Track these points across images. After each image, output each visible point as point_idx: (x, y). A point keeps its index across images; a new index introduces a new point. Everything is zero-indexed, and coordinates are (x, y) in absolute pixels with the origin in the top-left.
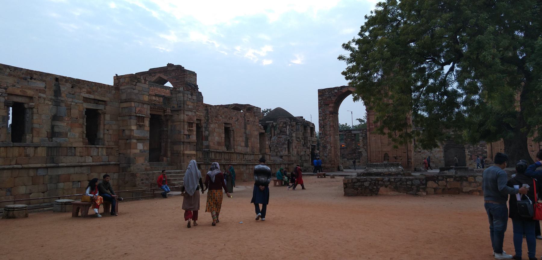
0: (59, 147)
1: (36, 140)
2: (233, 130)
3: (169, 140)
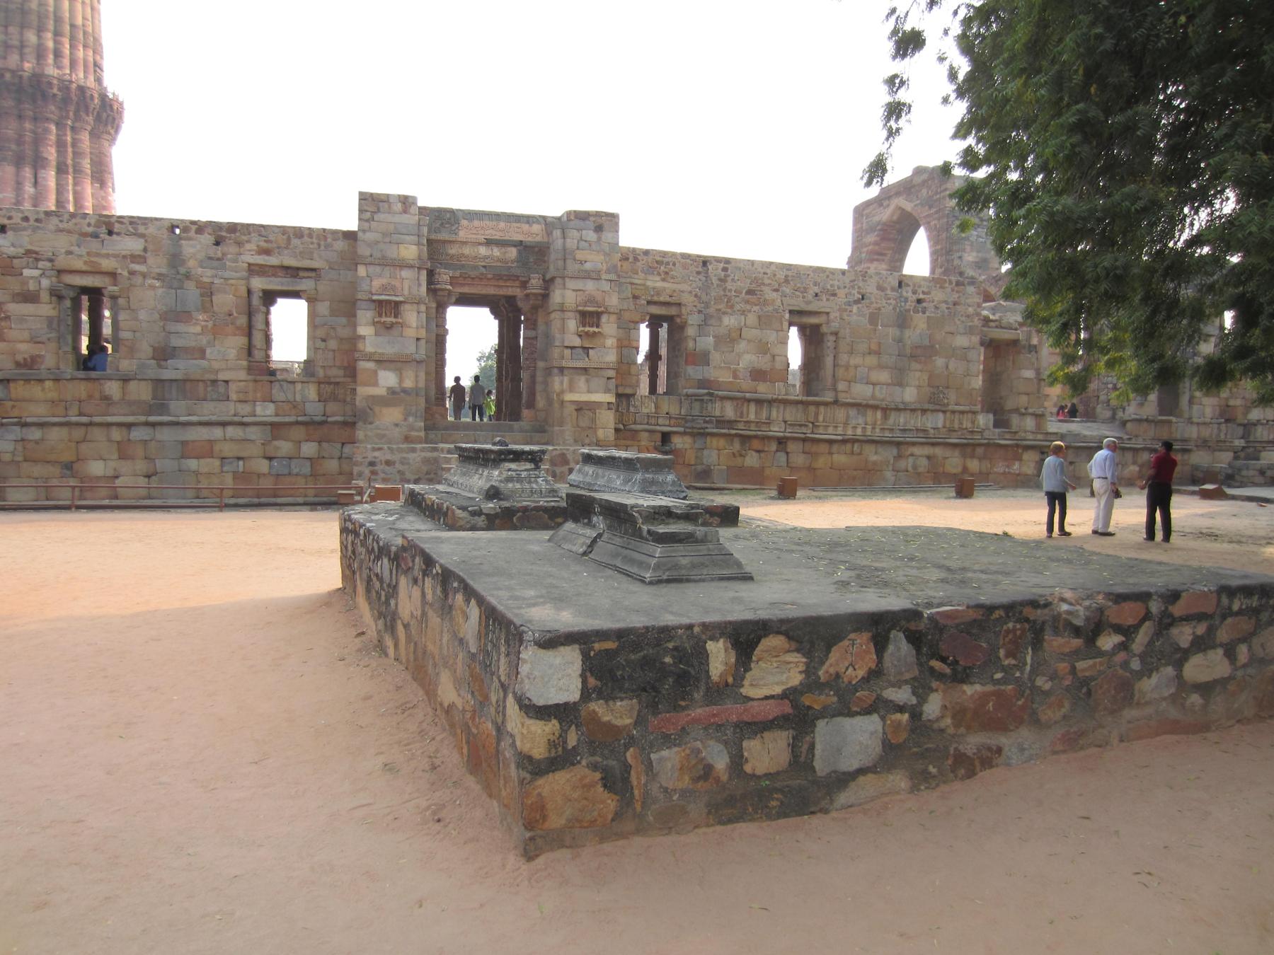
2: (836, 334)
3: (541, 364)
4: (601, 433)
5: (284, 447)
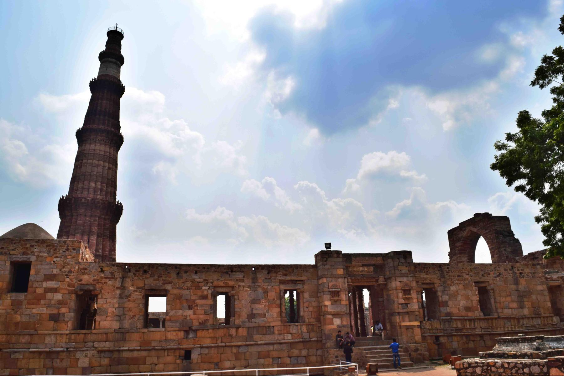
1: (237, 322)
2: (493, 290)
3: (387, 311)
4: (417, 338)
5: (296, 352)
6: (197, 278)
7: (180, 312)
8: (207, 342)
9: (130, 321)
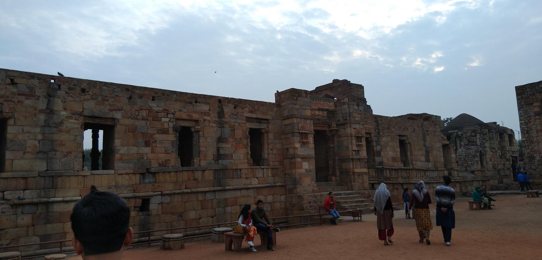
0: (225, 169)
1: (203, 163)
2: (410, 143)
3: (337, 158)
6: (154, 105)
7: (134, 150)
8: (169, 188)
9: (63, 160)
